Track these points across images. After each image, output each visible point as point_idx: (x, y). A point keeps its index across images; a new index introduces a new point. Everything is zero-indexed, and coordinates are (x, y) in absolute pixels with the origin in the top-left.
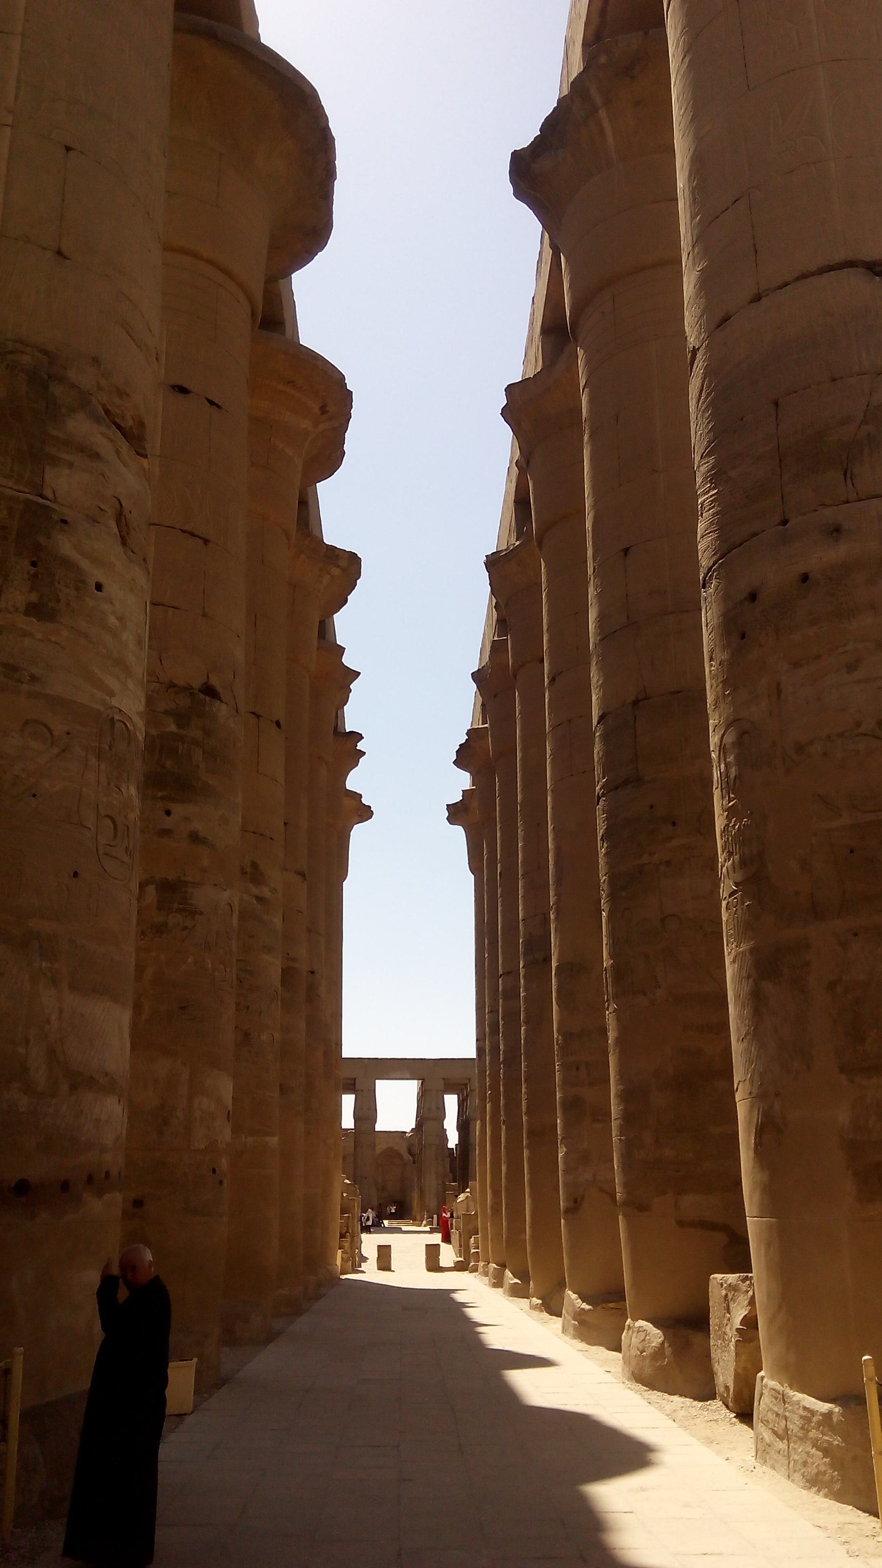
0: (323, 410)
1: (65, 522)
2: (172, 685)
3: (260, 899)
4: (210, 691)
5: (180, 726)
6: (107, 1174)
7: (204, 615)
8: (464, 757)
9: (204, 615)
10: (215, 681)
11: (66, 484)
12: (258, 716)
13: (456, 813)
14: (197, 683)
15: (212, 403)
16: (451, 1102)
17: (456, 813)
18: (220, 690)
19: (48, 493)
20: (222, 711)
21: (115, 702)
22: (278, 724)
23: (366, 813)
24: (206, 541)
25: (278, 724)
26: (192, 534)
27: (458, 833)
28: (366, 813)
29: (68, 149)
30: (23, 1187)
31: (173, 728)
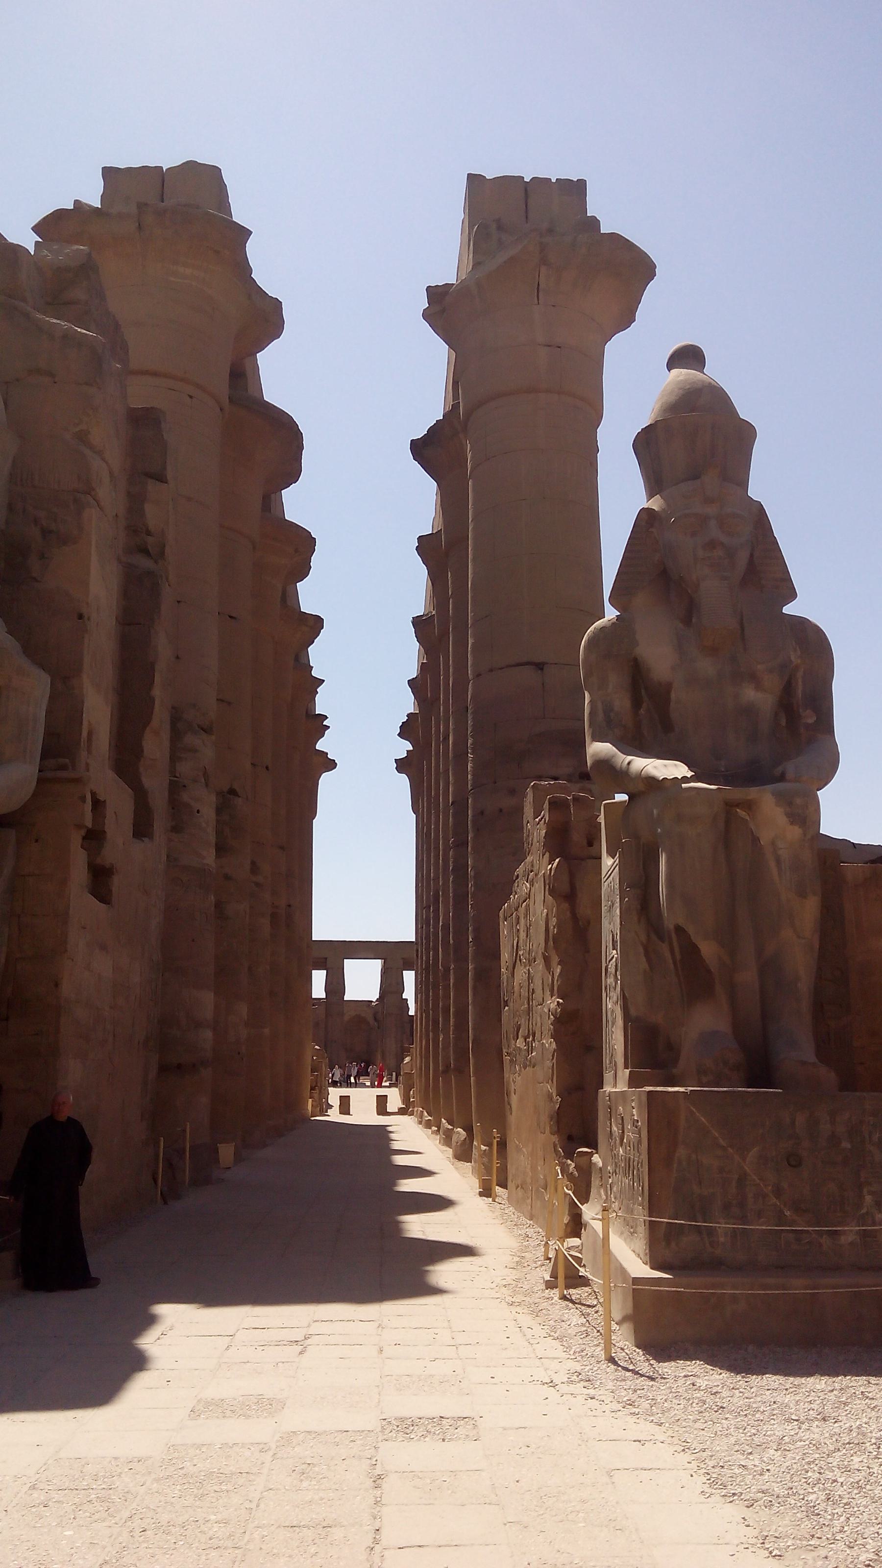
0: (296, 551)
1: (185, 786)
3: (257, 884)
4: (233, 792)
8: (405, 731)
13: (402, 765)
15: (230, 617)
16: (409, 977)
17: (402, 765)
18: (238, 790)
19: (178, 775)
20: (239, 801)
21: (205, 861)
22: (267, 768)
23: (331, 765)
24: (229, 703)
25: (267, 768)
27: (404, 779)
28: (331, 765)
29: (179, 602)
30: (179, 1066)
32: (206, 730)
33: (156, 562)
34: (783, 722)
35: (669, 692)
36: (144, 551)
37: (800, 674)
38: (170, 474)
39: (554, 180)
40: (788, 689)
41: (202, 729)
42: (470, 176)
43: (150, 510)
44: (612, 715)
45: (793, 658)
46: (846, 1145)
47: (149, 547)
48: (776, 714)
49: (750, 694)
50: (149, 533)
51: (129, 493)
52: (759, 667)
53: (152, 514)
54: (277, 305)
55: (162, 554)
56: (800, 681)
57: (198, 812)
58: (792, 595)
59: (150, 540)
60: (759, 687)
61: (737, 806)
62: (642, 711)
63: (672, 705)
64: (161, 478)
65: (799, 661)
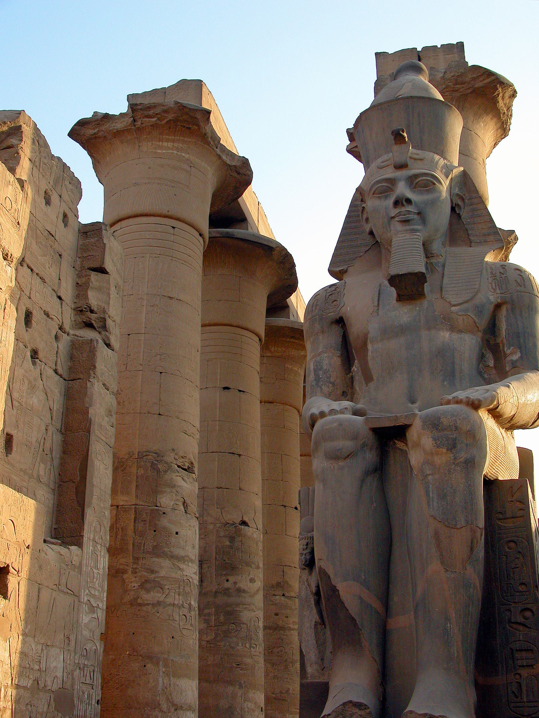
1: (164, 513)
4: (244, 523)
5: (230, 542)
7: (240, 489)
10: (246, 519)
12: (285, 506)
14: (238, 520)
15: (240, 391)
19: (158, 505)
22: (296, 508)
24: (240, 455)
29: (161, 373)
31: (228, 543)
34: (491, 363)
35: (365, 344)
36: (89, 325)
37: (504, 311)
38: (108, 265)
39: (439, 46)
42: (377, 54)
44: (321, 372)
45: (492, 298)
47: (93, 322)
49: (445, 335)
50: (92, 311)
52: (453, 308)
53: (94, 299)
54: (245, 162)
55: (104, 327)
56: (504, 320)
57: (177, 533)
59: (93, 316)
60: (452, 329)
62: (354, 368)
63: (370, 353)
64: (102, 270)
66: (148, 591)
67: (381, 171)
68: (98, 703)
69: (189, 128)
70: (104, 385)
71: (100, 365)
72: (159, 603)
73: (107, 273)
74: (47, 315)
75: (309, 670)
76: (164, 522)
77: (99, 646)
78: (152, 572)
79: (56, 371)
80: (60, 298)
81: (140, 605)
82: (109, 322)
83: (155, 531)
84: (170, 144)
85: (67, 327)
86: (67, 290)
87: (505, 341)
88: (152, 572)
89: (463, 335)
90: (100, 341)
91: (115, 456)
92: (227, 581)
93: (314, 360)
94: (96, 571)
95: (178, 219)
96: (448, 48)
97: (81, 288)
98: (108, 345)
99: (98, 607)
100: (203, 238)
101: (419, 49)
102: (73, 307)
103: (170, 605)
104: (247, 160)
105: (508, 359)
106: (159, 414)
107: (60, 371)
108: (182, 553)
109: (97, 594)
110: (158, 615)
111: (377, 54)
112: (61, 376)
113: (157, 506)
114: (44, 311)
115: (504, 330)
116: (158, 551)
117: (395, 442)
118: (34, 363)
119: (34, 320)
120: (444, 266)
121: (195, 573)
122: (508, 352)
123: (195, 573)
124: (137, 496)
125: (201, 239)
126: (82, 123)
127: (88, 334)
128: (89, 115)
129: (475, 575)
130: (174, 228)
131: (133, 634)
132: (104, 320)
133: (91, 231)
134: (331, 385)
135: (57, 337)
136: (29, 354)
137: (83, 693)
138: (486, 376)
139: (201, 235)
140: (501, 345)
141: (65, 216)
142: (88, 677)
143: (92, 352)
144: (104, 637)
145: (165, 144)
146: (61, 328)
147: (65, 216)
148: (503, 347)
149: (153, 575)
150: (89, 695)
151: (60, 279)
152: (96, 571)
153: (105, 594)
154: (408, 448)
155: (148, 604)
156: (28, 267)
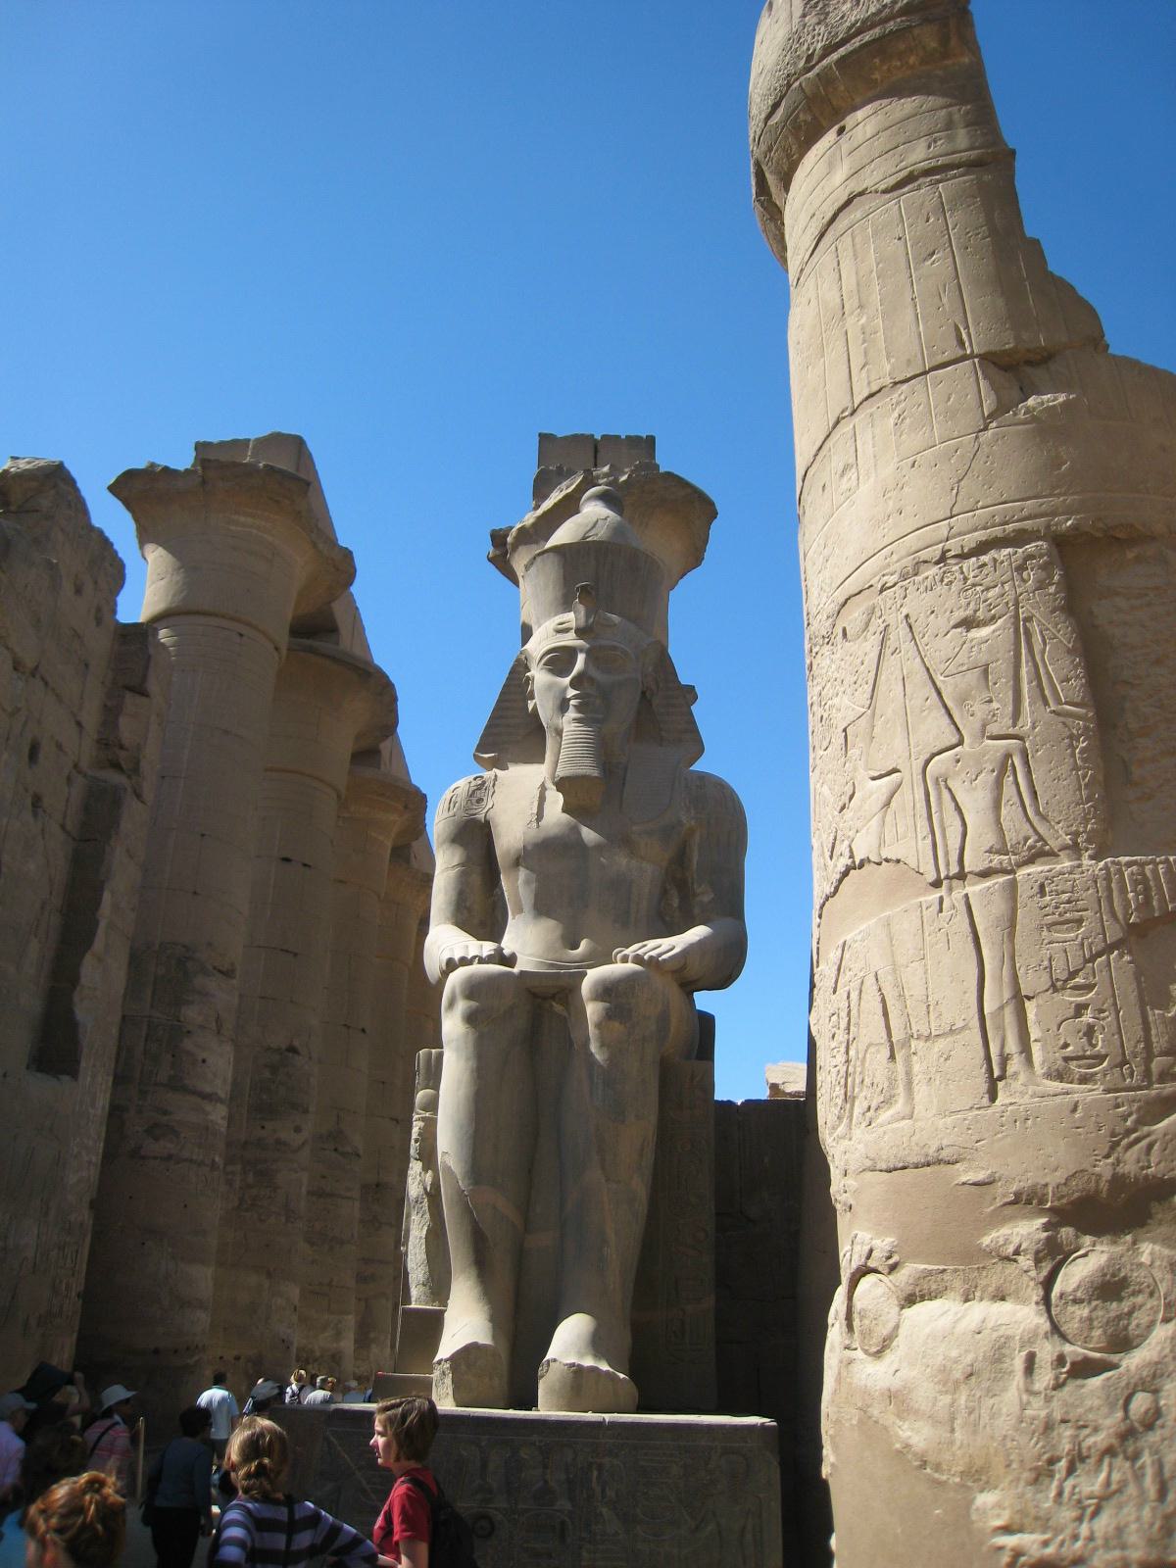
0: (406, 807)
1: (189, 1032)
2: (269, 1048)
4: (292, 1050)
6: (197, 1346)
7: (292, 1001)
9: (292, 1001)
10: (296, 1043)
11: (191, 1014)
12: (349, 1027)
15: (305, 865)
19: (182, 1019)
24: (296, 955)
25: (363, 1030)
26: (287, 951)
29: (203, 835)
32: (228, 974)
33: (129, 777)
34: (676, 902)
36: (116, 766)
38: (153, 686)
39: (623, 437)
40: (681, 858)
41: (220, 971)
42: (540, 435)
43: (123, 721)
45: (684, 819)
46: (563, 1504)
47: (123, 763)
48: (664, 892)
50: (122, 747)
51: (105, 706)
53: (127, 729)
54: (348, 554)
55: (136, 770)
57: (204, 1061)
58: (698, 749)
59: (122, 754)
61: (553, 997)
64: (143, 693)
65: (693, 822)
66: (156, 1139)
67: (559, 635)
68: (78, 1297)
69: (277, 502)
70: (128, 851)
71: (126, 825)
72: (170, 1157)
73: (147, 696)
74: (59, 746)
75: (414, 1292)
76: (187, 1044)
77: (85, 1216)
78: (165, 1113)
79: (63, 827)
80: (79, 724)
81: (143, 1158)
82: (144, 766)
83: (173, 1056)
84: (250, 520)
85: (84, 765)
86: (91, 718)
87: (695, 876)
88: (165, 1113)
89: (644, 864)
90: (129, 789)
91: (131, 948)
92: (263, 1127)
93: (445, 874)
94: (91, 1111)
95: (249, 624)
96: (634, 441)
97: (111, 714)
98: (139, 796)
99: (90, 1162)
100: (279, 653)
101: (598, 437)
102: (96, 737)
103: (186, 1160)
104: (351, 553)
105: (698, 899)
106: (195, 893)
107: (69, 827)
108: (208, 1089)
109: (91, 1143)
110: (167, 1174)
111: (540, 435)
112: (68, 833)
113: (179, 1021)
114: (57, 742)
115: (695, 863)
116: (176, 1085)
117: (552, 1006)
118: (35, 815)
119: (41, 756)
120: (626, 769)
121: (222, 1118)
122: (698, 891)
123: (222, 1118)
124: (152, 1006)
125: (276, 654)
126: (130, 475)
127: (115, 778)
128: (142, 465)
129: (640, 1187)
130: (241, 635)
131: (131, 1197)
132: (138, 763)
133: (138, 635)
134: (465, 912)
135: (69, 780)
136: (29, 801)
137: (61, 1282)
138: (667, 919)
139: (277, 649)
140: (690, 881)
141: (99, 609)
142: (69, 1261)
143: (117, 803)
144: (93, 1205)
145: (242, 519)
146: (76, 766)
147: (99, 609)
148: (693, 884)
149: (166, 1118)
150: (67, 1285)
151: (82, 698)
152: (91, 1111)
153: (102, 1145)
154: (570, 1014)
155: (155, 1158)
156: (43, 679)
